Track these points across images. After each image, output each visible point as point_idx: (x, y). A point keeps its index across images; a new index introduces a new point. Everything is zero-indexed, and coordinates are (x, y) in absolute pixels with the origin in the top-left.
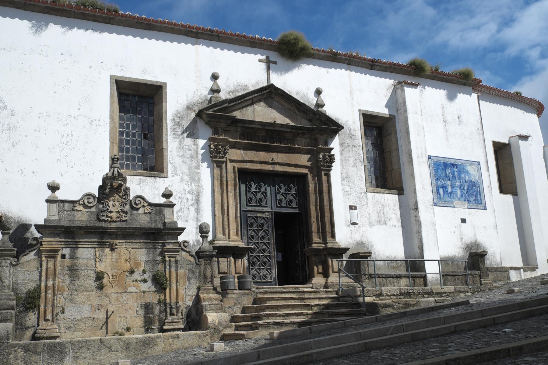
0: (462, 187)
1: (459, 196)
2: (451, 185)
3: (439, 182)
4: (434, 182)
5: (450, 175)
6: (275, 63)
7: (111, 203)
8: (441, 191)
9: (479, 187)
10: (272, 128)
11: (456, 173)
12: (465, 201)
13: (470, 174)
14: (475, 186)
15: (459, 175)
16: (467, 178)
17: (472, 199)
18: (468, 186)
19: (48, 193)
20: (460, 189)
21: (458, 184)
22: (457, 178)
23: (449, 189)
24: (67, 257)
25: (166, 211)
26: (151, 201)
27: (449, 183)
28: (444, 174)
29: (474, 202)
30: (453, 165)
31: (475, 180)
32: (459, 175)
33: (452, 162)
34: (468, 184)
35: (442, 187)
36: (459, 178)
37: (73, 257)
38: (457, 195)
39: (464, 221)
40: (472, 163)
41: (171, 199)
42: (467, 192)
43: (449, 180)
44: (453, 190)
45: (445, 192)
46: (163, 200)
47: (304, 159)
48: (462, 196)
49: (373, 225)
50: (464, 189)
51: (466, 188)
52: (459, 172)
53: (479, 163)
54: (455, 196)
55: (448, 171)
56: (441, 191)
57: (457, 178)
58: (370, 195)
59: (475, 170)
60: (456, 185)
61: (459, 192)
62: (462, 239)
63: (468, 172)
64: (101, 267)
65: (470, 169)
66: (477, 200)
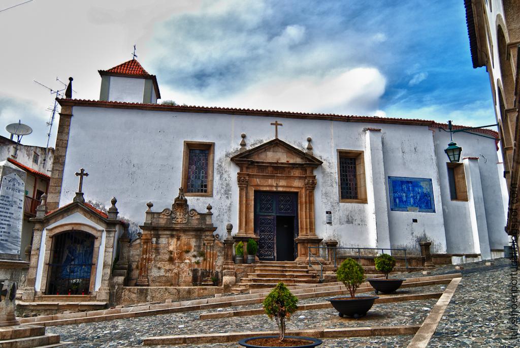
1: (412, 203)
2: (406, 196)
3: (396, 194)
4: (392, 194)
6: (281, 125)
7: (178, 213)
8: (397, 200)
9: (430, 196)
10: (275, 165)
12: (417, 207)
14: (427, 196)
15: (413, 188)
16: (420, 190)
17: (423, 206)
18: (420, 197)
19: (147, 209)
21: (412, 195)
23: (404, 199)
24: (154, 242)
25: (208, 218)
26: (199, 212)
27: (404, 194)
28: (401, 188)
29: (425, 207)
30: (408, 182)
33: (408, 180)
35: (398, 198)
37: (157, 243)
38: (410, 203)
39: (415, 221)
40: (424, 180)
41: (212, 211)
42: (419, 200)
43: (405, 193)
46: (206, 211)
47: (297, 183)
48: (415, 203)
49: (343, 224)
51: (418, 197)
52: (414, 187)
53: (431, 180)
54: (409, 204)
55: (404, 186)
56: (397, 200)
58: (341, 204)
59: (427, 185)
61: (412, 201)
62: (413, 233)
63: (421, 186)
64: (171, 248)
65: (422, 184)
66: (428, 206)
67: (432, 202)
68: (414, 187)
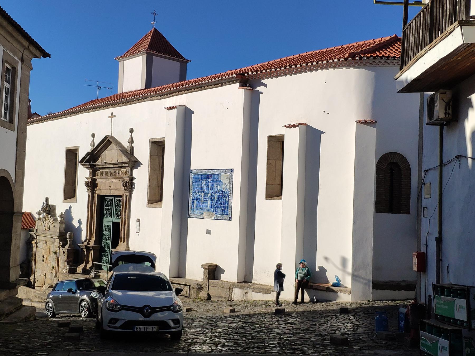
0: (213, 198)
5: (205, 187)
11: (210, 184)
13: (222, 183)
15: (212, 185)
20: (211, 199)
21: (210, 195)
22: (210, 189)
31: (226, 189)
32: (212, 185)
34: (218, 194)
36: (212, 189)
44: (205, 202)
45: (198, 204)
50: (214, 200)
57: (210, 189)
60: (208, 197)
67: (230, 204)
68: (213, 181)
